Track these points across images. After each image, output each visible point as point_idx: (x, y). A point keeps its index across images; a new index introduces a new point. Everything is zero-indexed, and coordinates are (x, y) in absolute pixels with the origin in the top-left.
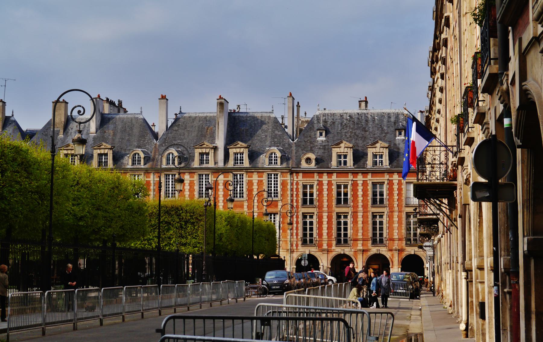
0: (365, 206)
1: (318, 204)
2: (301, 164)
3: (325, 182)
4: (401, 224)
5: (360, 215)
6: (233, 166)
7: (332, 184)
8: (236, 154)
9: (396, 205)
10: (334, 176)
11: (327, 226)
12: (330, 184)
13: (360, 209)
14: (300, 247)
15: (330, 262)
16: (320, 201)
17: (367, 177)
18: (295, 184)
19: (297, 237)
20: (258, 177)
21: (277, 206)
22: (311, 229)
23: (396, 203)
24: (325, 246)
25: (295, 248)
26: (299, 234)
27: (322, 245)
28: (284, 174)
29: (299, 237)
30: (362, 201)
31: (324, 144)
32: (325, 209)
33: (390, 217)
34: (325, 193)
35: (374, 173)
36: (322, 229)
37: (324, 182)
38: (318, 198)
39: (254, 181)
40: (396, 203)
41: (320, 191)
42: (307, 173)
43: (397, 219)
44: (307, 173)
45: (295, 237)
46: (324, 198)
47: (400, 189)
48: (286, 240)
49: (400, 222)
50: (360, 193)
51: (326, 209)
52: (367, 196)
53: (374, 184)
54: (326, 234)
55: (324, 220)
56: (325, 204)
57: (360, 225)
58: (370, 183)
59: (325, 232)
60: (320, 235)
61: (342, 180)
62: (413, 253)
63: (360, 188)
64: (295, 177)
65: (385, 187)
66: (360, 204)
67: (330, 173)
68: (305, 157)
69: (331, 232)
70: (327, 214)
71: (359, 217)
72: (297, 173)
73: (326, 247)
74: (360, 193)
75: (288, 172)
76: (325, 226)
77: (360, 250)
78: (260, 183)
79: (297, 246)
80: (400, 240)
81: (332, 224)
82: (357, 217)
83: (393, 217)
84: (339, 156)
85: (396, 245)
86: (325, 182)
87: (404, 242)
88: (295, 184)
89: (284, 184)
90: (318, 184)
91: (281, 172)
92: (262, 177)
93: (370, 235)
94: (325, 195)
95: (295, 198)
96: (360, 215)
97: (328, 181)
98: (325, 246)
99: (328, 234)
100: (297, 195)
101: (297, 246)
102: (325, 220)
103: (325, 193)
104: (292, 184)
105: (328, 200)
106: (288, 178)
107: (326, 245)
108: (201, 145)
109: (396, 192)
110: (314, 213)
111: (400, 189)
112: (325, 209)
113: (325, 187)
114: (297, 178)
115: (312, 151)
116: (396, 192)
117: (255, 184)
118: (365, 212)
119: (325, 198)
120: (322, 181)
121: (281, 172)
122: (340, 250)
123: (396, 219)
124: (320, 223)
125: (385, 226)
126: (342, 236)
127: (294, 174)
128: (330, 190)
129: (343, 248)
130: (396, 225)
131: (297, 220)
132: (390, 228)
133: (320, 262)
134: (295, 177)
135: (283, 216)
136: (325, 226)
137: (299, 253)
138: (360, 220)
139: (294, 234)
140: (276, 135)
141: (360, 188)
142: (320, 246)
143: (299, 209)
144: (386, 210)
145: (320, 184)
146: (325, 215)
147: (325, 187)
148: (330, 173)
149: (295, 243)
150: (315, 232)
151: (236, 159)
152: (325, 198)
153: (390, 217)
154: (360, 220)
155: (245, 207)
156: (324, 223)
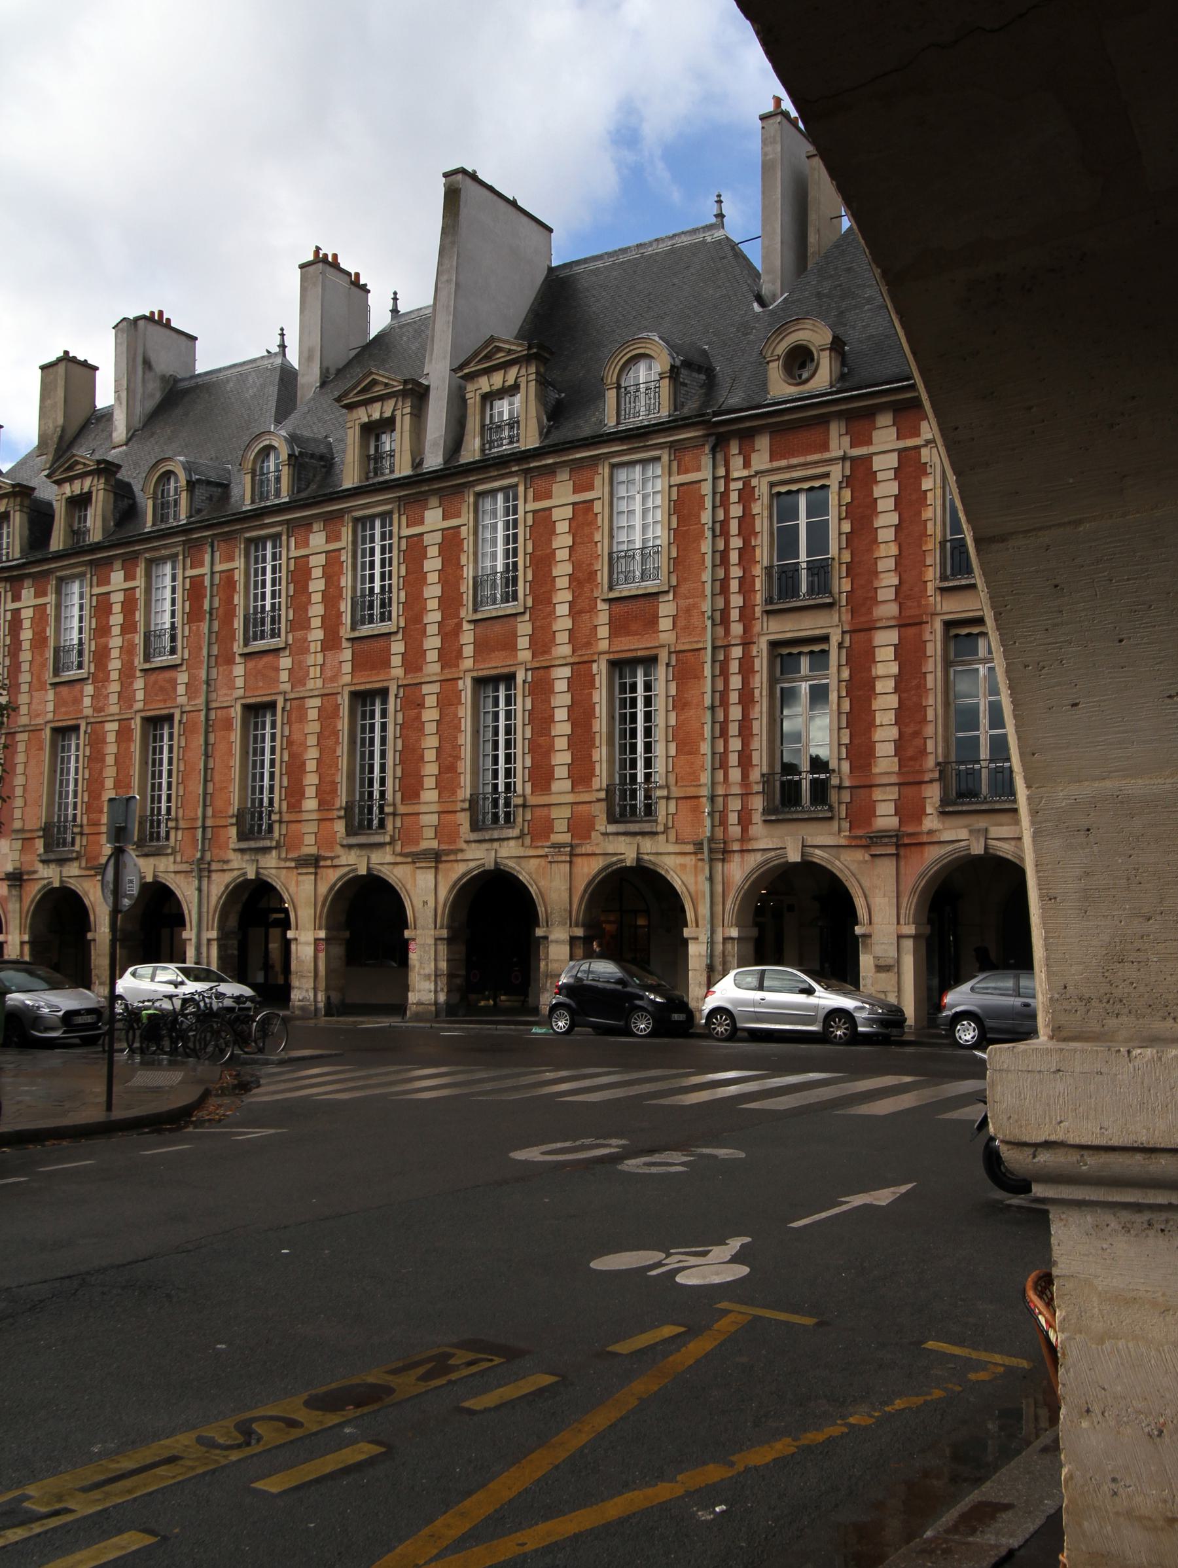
1: (846, 586)
3: (885, 464)
7: (922, 470)
11: (893, 701)
14: (758, 828)
15: (909, 903)
16: (862, 570)
19: (745, 776)
21: (652, 621)
24: (886, 817)
25: (735, 831)
26: (755, 759)
27: (869, 811)
29: (755, 775)
34: (886, 519)
36: (871, 725)
37: (878, 463)
38: (846, 557)
41: (861, 514)
45: (735, 774)
46: (882, 551)
48: (691, 792)
51: (893, 609)
54: (890, 749)
55: (880, 670)
64: (737, 462)
68: (782, 348)
69: (917, 733)
70: (892, 636)
72: (747, 436)
73: (893, 822)
75: (694, 445)
79: (745, 820)
81: (921, 688)
86: (885, 464)
88: (734, 497)
90: (848, 481)
91: (671, 445)
92: (590, 487)
94: (886, 535)
95: (736, 572)
97: (901, 451)
98: (886, 817)
99: (900, 745)
100: (746, 553)
101: (745, 820)
102: (886, 666)
103: (886, 519)
104: (722, 500)
105: (899, 559)
107: (890, 808)
108: (365, 390)
110: (825, 639)
113: (886, 490)
114: (747, 464)
119: (887, 551)
120: (868, 459)
121: (671, 445)
122: (963, 834)
127: (734, 449)
129: (981, 822)
131: (745, 682)
133: (859, 903)
134: (737, 462)
135: (685, 673)
137: (753, 860)
139: (733, 759)
142: (861, 814)
143: (757, 627)
145: (860, 475)
146: (885, 642)
147: (886, 490)
149: (735, 804)
152: (887, 551)
156: (880, 687)
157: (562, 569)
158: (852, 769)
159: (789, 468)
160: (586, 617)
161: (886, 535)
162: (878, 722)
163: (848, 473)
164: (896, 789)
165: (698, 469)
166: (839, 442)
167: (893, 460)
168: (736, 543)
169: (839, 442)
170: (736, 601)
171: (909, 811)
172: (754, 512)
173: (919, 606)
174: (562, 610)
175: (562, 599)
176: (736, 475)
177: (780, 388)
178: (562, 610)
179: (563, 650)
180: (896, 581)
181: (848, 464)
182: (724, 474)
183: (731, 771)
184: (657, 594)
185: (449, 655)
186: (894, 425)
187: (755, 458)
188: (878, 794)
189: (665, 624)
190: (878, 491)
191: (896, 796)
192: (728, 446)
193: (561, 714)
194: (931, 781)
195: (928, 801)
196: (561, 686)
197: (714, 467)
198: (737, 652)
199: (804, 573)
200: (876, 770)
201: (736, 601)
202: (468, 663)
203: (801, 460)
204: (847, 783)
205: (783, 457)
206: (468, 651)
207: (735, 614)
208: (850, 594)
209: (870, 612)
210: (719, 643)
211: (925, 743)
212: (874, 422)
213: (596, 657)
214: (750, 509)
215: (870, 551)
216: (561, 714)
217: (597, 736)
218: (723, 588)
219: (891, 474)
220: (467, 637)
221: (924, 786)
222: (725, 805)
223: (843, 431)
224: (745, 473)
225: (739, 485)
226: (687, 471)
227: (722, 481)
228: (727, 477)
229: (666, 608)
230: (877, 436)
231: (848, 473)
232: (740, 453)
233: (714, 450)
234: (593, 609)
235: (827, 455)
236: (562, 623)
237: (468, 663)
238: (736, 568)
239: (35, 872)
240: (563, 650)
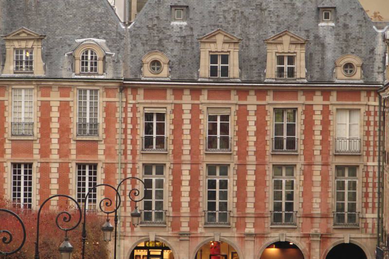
0: (260, 154)
2: (141, 72)
3: (187, 108)
4: (327, 186)
5: (251, 169)
6: (12, 75)
7: (200, 112)
8: (18, 51)
9: (317, 153)
10: (204, 98)
11: (188, 189)
12: (195, 110)
13: (252, 158)
16: (178, 142)
17: (265, 99)
18: (129, 110)
20: (61, 96)
22: (160, 194)
23: (317, 149)
24: (185, 228)
28: (110, 92)
30: (256, 143)
31: (184, 33)
32: (186, 157)
33: (308, 175)
34: (187, 126)
35: (279, 92)
36: (180, 195)
37: (184, 107)
39: (52, 104)
40: (317, 149)
41: (178, 123)
42: (154, 90)
43: (319, 178)
44: (154, 90)
46: (184, 137)
47: (326, 123)
49: (324, 183)
50: (252, 128)
51: (188, 158)
52: (265, 133)
53: (279, 112)
54: (187, 205)
55: (183, 178)
56: (186, 148)
57: (251, 188)
58: (270, 109)
59: (185, 200)
60: (177, 206)
61: (219, 102)
62: (347, 241)
63: (252, 119)
64: (130, 97)
65: (300, 118)
66: (252, 149)
67: (196, 91)
69: (197, 200)
70: (188, 167)
71: (249, 172)
72: (135, 89)
74: (252, 128)
76: (185, 189)
77: (250, 235)
78: (64, 108)
80: (324, 216)
82: (245, 173)
83: (311, 175)
84: (214, 59)
85: (317, 228)
87: (332, 221)
88: (129, 110)
89: (109, 109)
90: (173, 111)
93: (270, 207)
96: (251, 169)
98: (185, 228)
99: (190, 204)
100: (134, 131)
102: (186, 177)
103: (187, 126)
105: (191, 141)
106: (116, 98)
107: (186, 224)
109: (318, 128)
111: (326, 123)
112: (186, 157)
113: (187, 116)
114: (134, 99)
115: (161, 46)
116: (318, 128)
117: (55, 109)
118: (261, 163)
119: (186, 138)
120: (181, 105)
123: (317, 178)
124: (177, 183)
125: (359, 191)
126: (217, 208)
127: (129, 92)
128: (195, 122)
130: (317, 189)
132: (307, 194)
136: (185, 189)
138: (251, 178)
140: (93, 13)
141: (252, 119)
142: (176, 226)
143: (138, 158)
144: (300, 162)
146: (186, 170)
147: (187, 116)
148: (196, 91)
150: (167, 200)
151: (18, 62)
152: (186, 138)
153: (308, 175)
154: (251, 178)
155: (36, 151)
156: (184, 183)
157: (55, 125)
158: (173, 210)
159: (151, 103)
160: (65, 145)
161: (187, 132)
162: (183, 195)
163: (173, 108)
164: (189, 218)
165: (115, 97)
166: (234, 98)
167: (189, 107)
168: (130, 126)
169: (170, 98)
170: (130, 147)
171: (193, 226)
172: (137, 116)
173: (198, 158)
174: (55, 141)
175: (55, 137)
176: (130, 102)
177: (340, 77)
178: (55, 141)
179: (54, 156)
180: (189, 148)
181: (173, 105)
182: (125, 101)
183: (127, 208)
184: (97, 141)
185: (64, 153)
186: (255, 95)
187: (137, 96)
188: (247, 220)
189: (101, 152)
190: (184, 116)
191: (188, 220)
192: (127, 90)
193: (54, 181)
194: (201, 217)
195: (200, 223)
196: (54, 170)
197: (122, 98)
198: (130, 166)
199: (218, 140)
200: (181, 211)
201: (130, 147)
202: (74, 157)
203: (156, 101)
204: (236, 216)
205: (149, 99)
206: (9, 151)
207: (129, 152)
208: (173, 151)
209: (180, 157)
210: (123, 162)
211: (199, 204)
212: (183, 92)
213: (70, 161)
214: (136, 115)
215: (181, 136)
216: (54, 181)
217: (71, 191)
218: (125, 142)
219: (189, 111)
220: (73, 146)
221: (198, 218)
222: (125, 220)
223: (172, 94)
224: (134, 102)
225: (131, 106)
226: (109, 97)
227: (124, 103)
228: (126, 102)
229: (101, 147)
230: (184, 97)
231: (173, 108)
232: (132, 94)
233: (121, 91)
234: (68, 141)
235: (360, 103)
236: (55, 145)
237: (8, 156)
238: (130, 135)
239: (333, 234)
240: (54, 156)
